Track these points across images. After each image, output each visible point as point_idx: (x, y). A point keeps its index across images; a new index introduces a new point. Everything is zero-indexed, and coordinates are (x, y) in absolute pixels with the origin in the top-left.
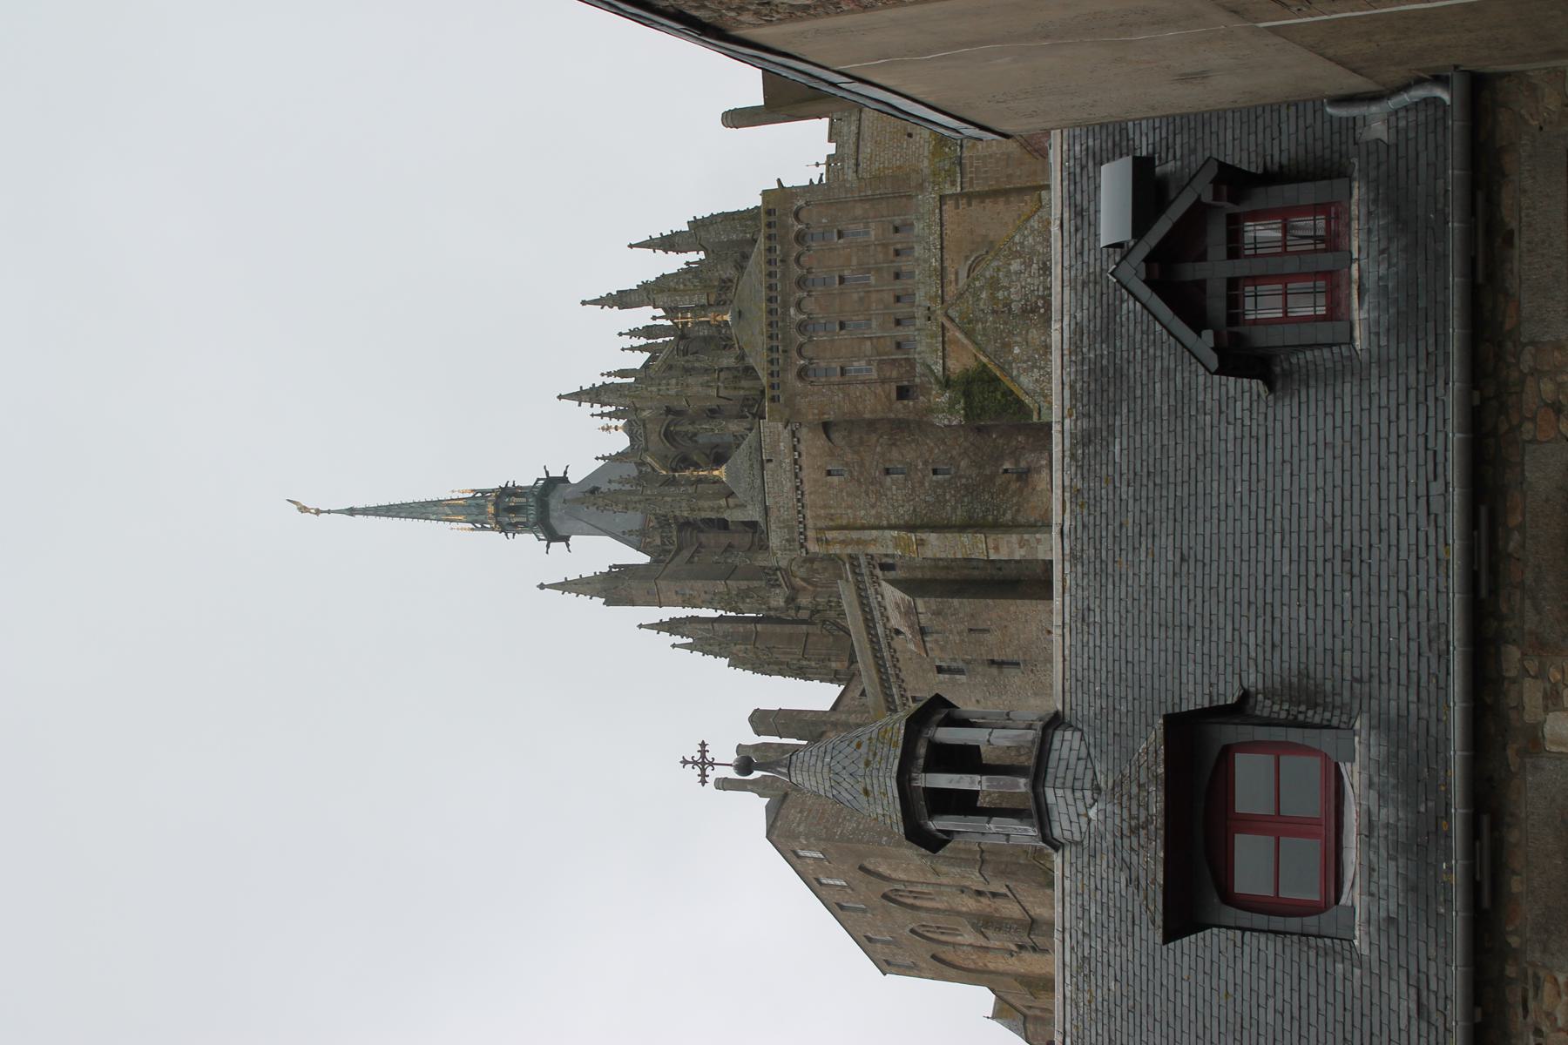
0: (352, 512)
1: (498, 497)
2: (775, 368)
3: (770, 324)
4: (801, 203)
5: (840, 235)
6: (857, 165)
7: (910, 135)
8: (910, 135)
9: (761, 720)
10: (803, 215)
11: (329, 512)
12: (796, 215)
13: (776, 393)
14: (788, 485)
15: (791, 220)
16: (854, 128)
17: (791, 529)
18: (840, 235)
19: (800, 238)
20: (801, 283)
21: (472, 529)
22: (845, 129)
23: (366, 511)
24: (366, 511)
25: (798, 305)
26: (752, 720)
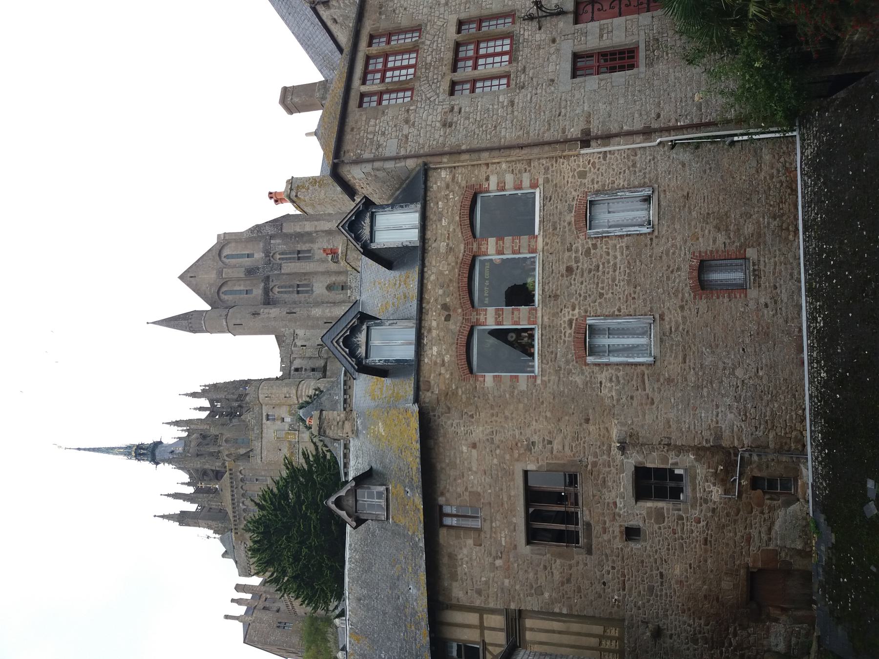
2: (236, 523)
3: (233, 508)
4: (242, 468)
5: (257, 480)
6: (262, 458)
7: (280, 450)
8: (280, 450)
9: (239, 588)
10: (243, 472)
12: (240, 472)
13: (237, 531)
14: (243, 555)
15: (239, 474)
16: (260, 444)
17: (245, 569)
18: (257, 480)
19: (242, 480)
20: (243, 495)
22: (257, 444)
25: (243, 503)
26: (236, 588)
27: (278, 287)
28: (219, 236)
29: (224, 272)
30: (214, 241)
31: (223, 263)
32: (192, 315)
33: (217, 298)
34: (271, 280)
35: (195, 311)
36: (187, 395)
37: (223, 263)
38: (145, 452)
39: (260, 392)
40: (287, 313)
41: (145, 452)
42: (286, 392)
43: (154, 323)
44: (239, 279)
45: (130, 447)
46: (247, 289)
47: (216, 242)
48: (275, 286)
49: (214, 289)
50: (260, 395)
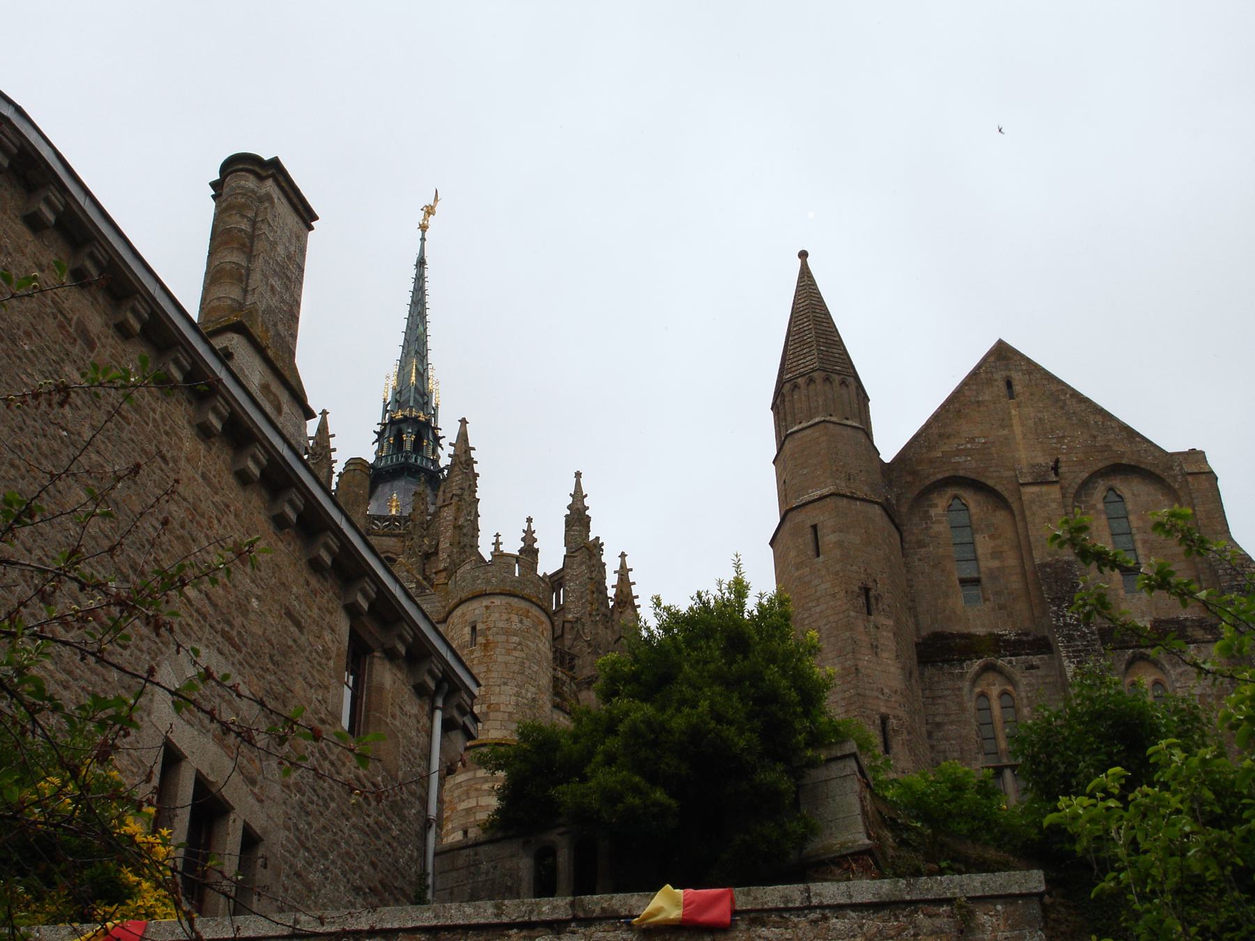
0: (421, 263)
1: (416, 419)
11: (423, 239)
21: (385, 401)
23: (420, 280)
24: (420, 280)
27: (1004, 693)
28: (1196, 456)
29: (1044, 488)
30: (1171, 440)
31: (1086, 486)
32: (843, 383)
33: (933, 479)
34: (1035, 660)
35: (862, 398)
36: (578, 495)
37: (1086, 486)
38: (408, 447)
39: (497, 601)
40: (884, 720)
41: (408, 447)
42: (494, 700)
43: (805, 274)
44: (1023, 547)
45: (427, 403)
46: (984, 580)
47: (1169, 451)
48: (1010, 680)
49: (967, 465)
50: (486, 602)
